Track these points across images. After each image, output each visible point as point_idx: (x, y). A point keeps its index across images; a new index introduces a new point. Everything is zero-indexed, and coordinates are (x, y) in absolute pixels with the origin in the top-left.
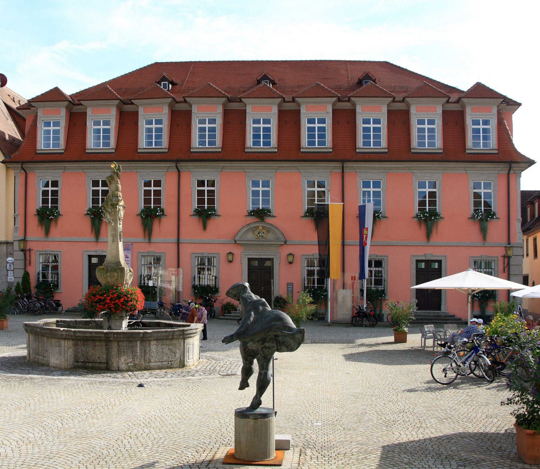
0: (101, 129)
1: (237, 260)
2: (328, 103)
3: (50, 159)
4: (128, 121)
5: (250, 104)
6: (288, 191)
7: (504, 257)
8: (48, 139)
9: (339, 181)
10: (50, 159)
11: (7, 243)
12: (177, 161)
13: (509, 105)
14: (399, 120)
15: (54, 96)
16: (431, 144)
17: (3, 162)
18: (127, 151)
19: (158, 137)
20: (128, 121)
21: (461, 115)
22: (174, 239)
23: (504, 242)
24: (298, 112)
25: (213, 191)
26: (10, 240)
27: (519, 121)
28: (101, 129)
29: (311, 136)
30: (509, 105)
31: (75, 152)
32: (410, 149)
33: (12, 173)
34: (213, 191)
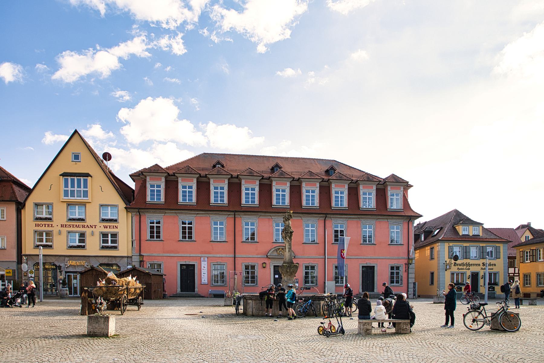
0: (188, 191)
1: (268, 267)
2: (288, 181)
3: (155, 208)
4: (203, 186)
5: (180, 177)
6: (270, 229)
7: (406, 264)
8: (153, 195)
9: (323, 224)
10: (155, 208)
11: (128, 257)
12: (236, 211)
13: (407, 186)
14: (354, 193)
15: (156, 170)
16: (313, 204)
17: (126, 208)
18: (203, 205)
19: (313, 200)
20: (203, 186)
21: (299, 188)
22: (233, 256)
23: (406, 257)
24: (240, 184)
25: (159, 227)
26: (130, 255)
27: (411, 194)
28: (188, 191)
29: (184, 196)
30: (407, 186)
31: (171, 204)
32: (272, 205)
33: (130, 215)
34: (159, 227)
